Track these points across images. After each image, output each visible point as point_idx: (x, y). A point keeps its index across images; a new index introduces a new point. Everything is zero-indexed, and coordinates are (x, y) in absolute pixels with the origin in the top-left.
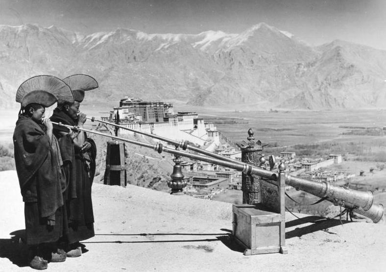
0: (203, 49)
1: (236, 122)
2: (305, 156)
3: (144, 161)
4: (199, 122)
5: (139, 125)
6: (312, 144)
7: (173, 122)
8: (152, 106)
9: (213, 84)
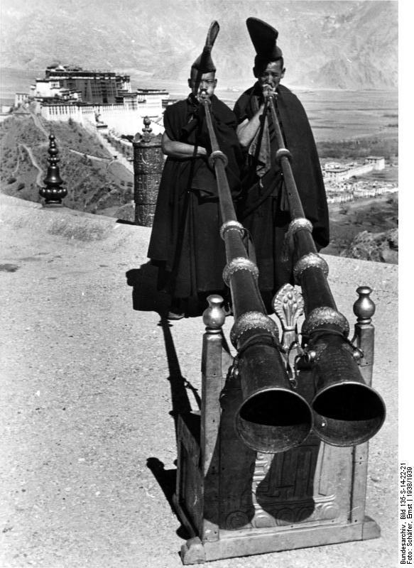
2: (332, 159)
3: (85, 163)
5: (76, 107)
6: (342, 141)
7: (131, 103)
9: (194, 47)
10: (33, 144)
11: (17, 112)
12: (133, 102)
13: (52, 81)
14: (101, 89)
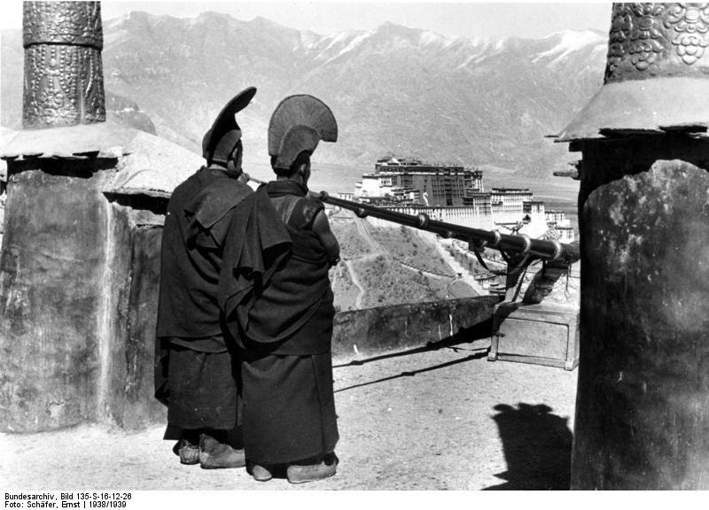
0: (551, 66)
3: (419, 282)
4: (534, 208)
7: (482, 206)
10: (355, 256)
11: (337, 215)
12: (485, 204)
13: (382, 177)
14: (444, 188)
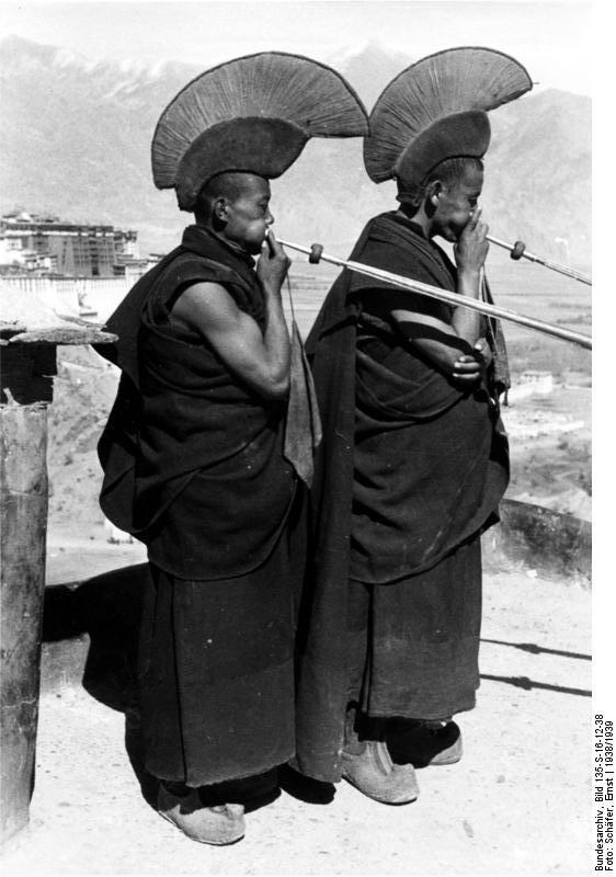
1: (298, 285)
5: (47, 281)
8: (84, 234)
13: (10, 237)
